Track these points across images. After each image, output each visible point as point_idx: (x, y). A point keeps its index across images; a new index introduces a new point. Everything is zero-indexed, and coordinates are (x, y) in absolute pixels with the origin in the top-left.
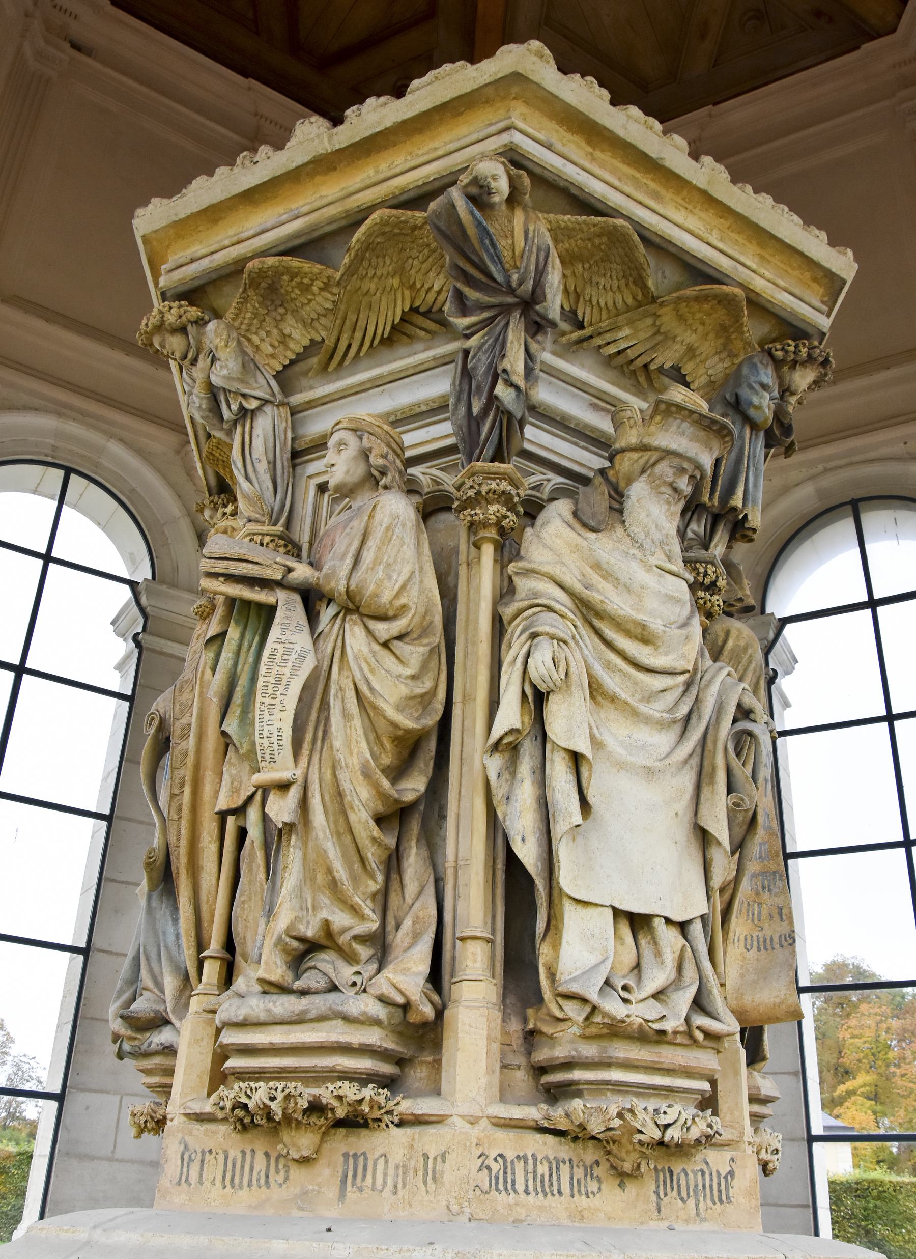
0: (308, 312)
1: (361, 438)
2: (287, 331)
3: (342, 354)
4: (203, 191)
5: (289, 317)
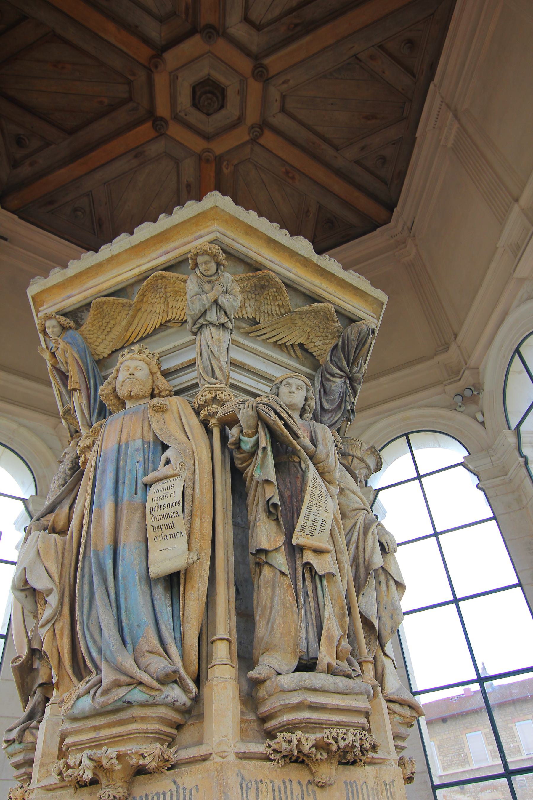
0: (265, 307)
1: (307, 390)
2: (247, 305)
4: (251, 217)
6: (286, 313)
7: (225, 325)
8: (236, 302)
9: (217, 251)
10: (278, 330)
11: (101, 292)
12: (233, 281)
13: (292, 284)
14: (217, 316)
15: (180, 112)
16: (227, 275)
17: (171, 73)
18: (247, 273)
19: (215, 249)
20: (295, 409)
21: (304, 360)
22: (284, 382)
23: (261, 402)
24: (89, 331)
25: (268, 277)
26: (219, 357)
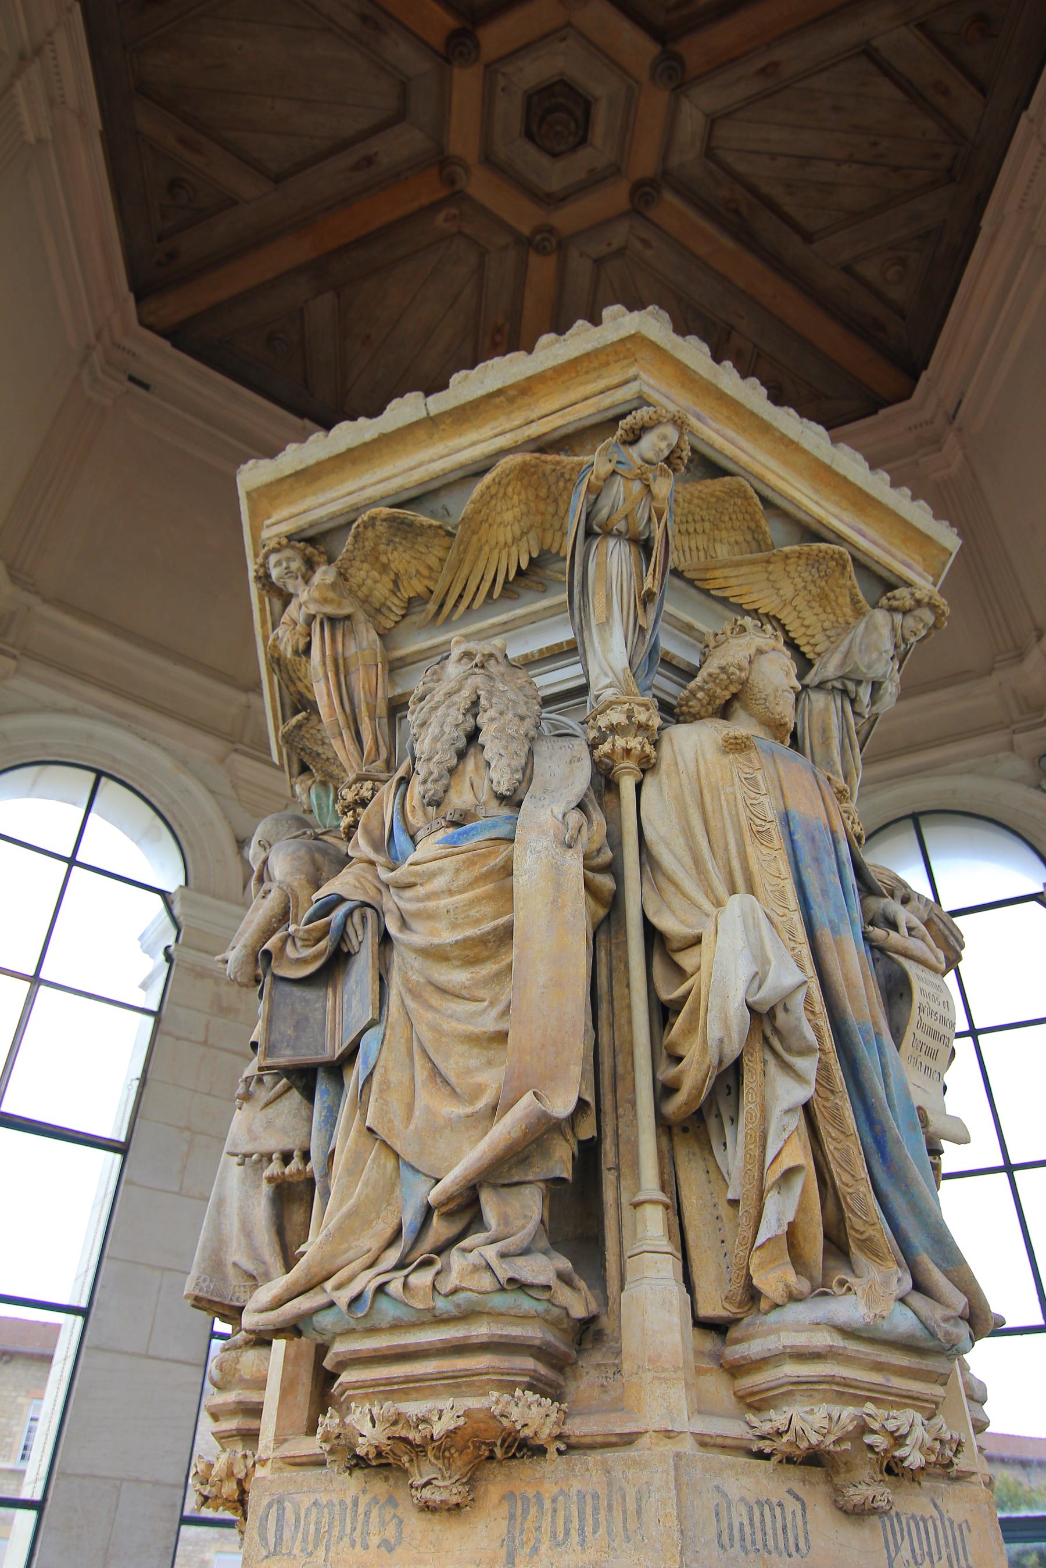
11: (761, 479)
15: (504, 74)
17: (569, 24)
24: (675, 501)
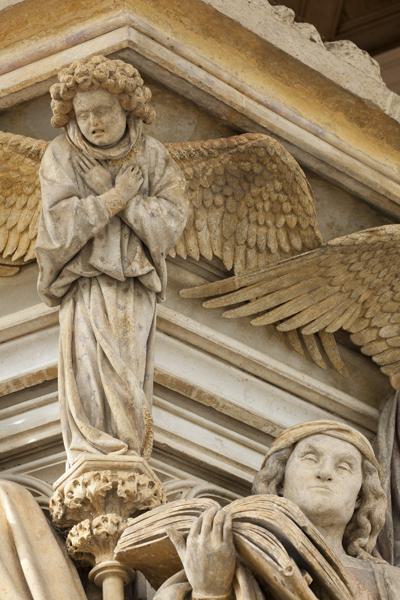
0: (249, 231)
1: (366, 471)
2: (201, 223)
3: (234, 302)
5: (218, 213)
6: (305, 248)
7: (143, 281)
8: (177, 218)
9: (132, 81)
10: (282, 293)
12: (167, 161)
13: (324, 170)
14: (122, 257)
16: (152, 143)
18: (205, 138)
19: (125, 74)
20: (332, 525)
21: (347, 375)
22: (302, 447)
23: (247, 515)
25: (262, 153)
26: (124, 373)
